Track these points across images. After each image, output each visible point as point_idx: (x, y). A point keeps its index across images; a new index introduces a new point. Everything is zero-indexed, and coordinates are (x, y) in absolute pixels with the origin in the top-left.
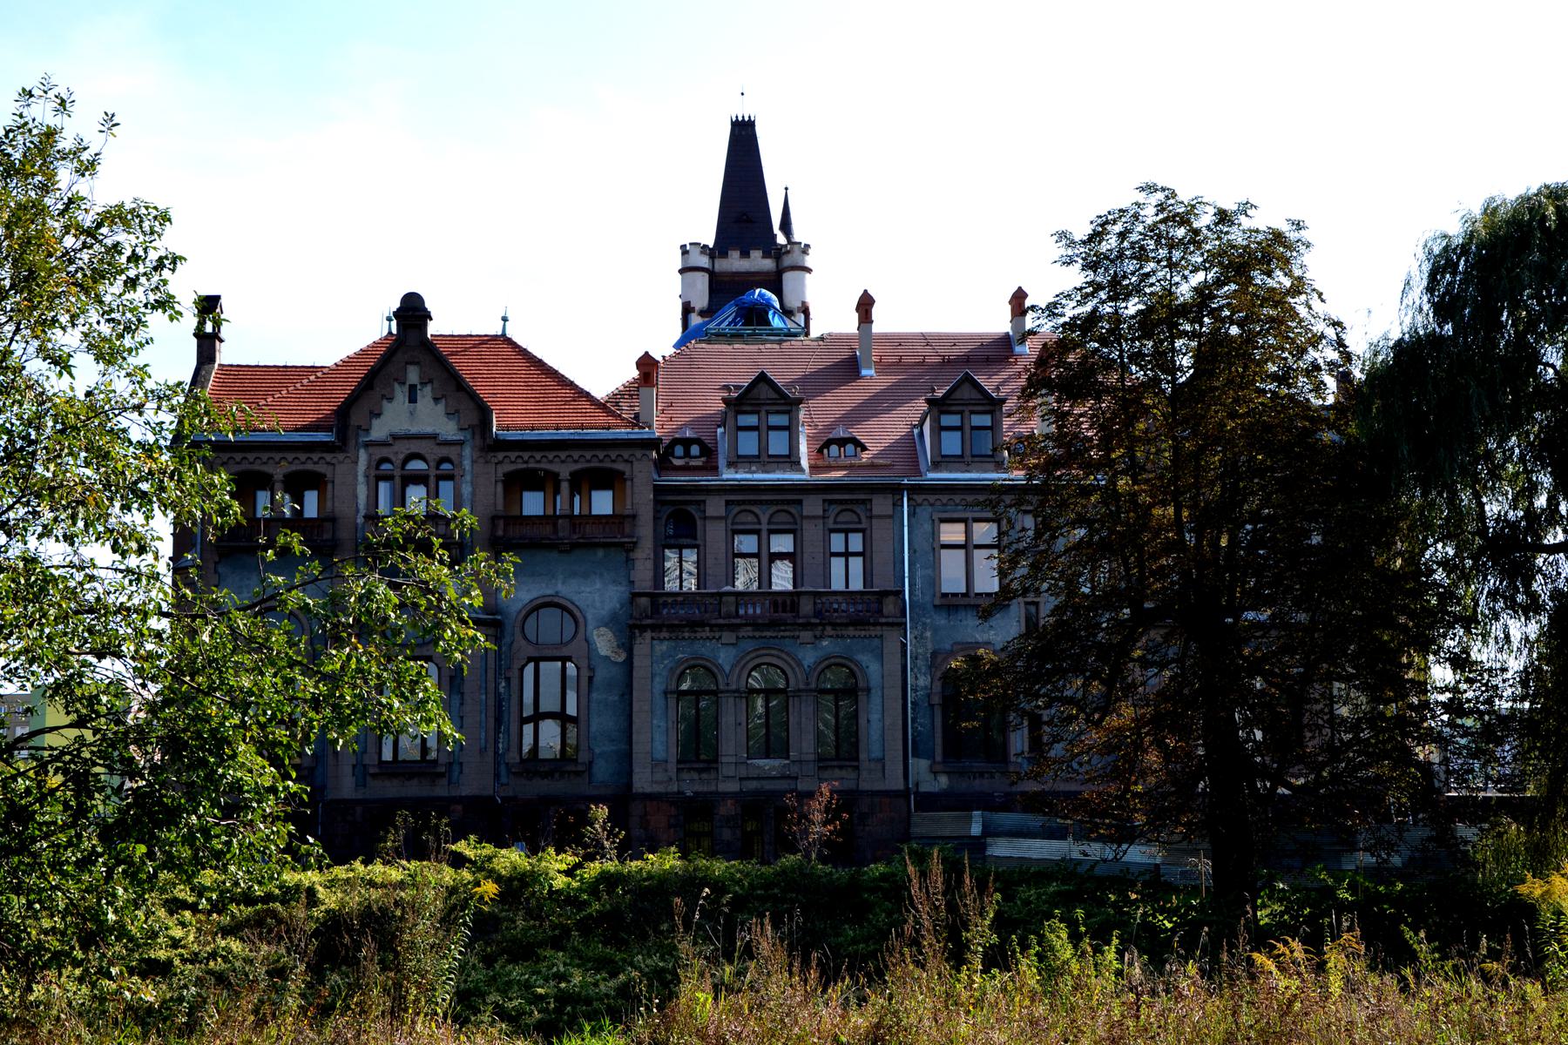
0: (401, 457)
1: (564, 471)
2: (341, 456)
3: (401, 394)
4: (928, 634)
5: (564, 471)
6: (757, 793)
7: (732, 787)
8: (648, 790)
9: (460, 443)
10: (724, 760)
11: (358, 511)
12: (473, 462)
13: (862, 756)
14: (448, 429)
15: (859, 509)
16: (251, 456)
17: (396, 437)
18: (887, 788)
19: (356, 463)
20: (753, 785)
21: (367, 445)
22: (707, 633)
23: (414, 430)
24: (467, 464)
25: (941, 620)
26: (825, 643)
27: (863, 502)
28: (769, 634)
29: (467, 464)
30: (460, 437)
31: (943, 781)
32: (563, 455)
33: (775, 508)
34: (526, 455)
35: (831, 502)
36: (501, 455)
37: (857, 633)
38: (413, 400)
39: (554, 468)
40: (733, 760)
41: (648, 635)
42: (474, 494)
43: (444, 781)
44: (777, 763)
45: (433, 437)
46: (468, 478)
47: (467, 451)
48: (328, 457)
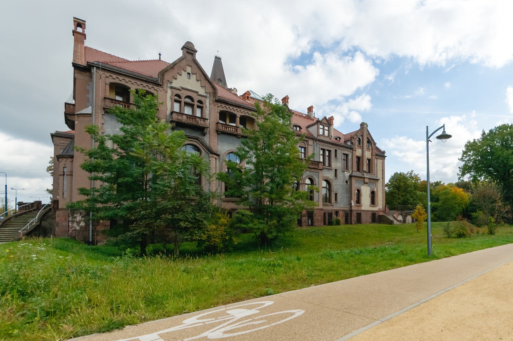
0: (185, 96)
1: (239, 115)
2: (161, 89)
5: (239, 115)
9: (206, 97)
11: (167, 109)
12: (210, 104)
14: (202, 92)
15: (305, 142)
16: (121, 78)
17: (183, 88)
19: (167, 92)
21: (171, 88)
23: (189, 88)
24: (208, 104)
27: (306, 141)
29: (208, 104)
30: (205, 94)
32: (239, 110)
34: (227, 107)
36: (219, 104)
39: (235, 112)
42: (210, 114)
45: (197, 92)
46: (208, 108)
47: (208, 101)
48: (156, 88)
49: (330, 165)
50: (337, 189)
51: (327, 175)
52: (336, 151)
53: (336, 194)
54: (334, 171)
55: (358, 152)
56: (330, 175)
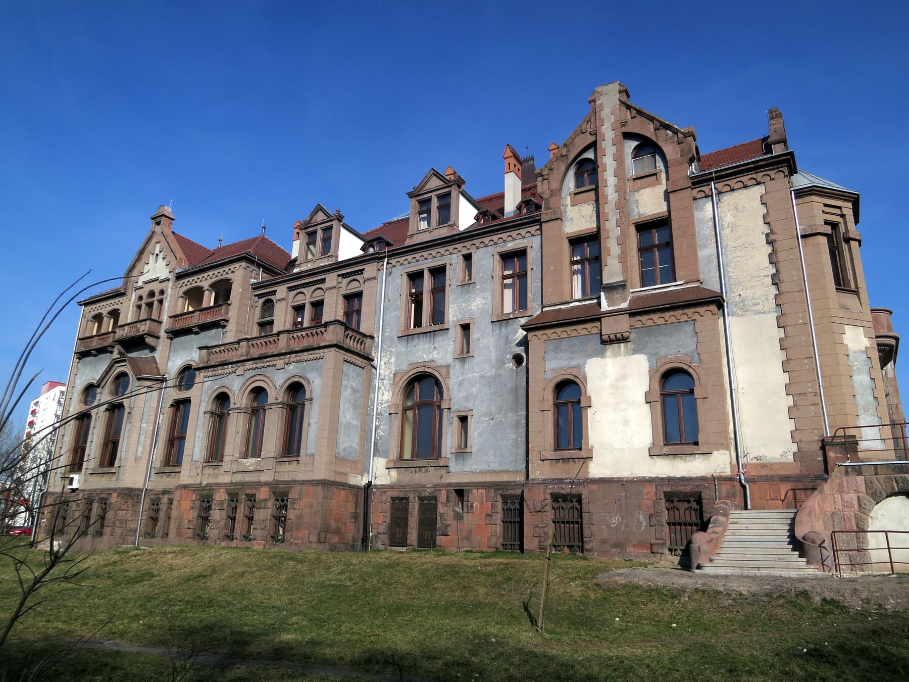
1: (206, 284)
2: (125, 298)
3: (152, 258)
4: (393, 360)
5: (206, 284)
6: (236, 484)
7: (226, 479)
8: (186, 483)
9: (168, 280)
10: (225, 459)
13: (302, 452)
17: (146, 283)
18: (315, 478)
20: (238, 478)
22: (229, 369)
25: (402, 347)
26: (291, 367)
28: (260, 365)
31: (394, 473)
33: (314, 288)
35: (344, 276)
37: (309, 357)
38: (156, 260)
40: (230, 458)
41: (203, 373)
43: (114, 478)
44: (253, 460)
45: (156, 280)
49: (438, 316)
50: (467, 399)
51: (427, 358)
52: (468, 258)
53: (463, 419)
54: (455, 333)
55: (578, 218)
56: (437, 352)
